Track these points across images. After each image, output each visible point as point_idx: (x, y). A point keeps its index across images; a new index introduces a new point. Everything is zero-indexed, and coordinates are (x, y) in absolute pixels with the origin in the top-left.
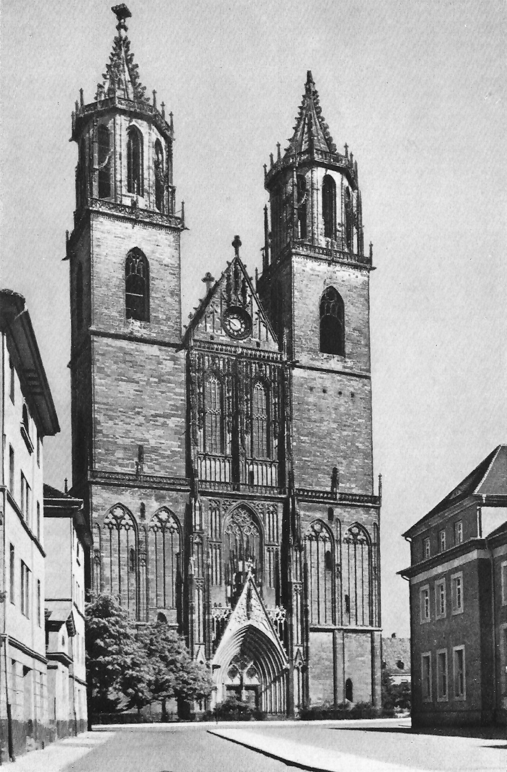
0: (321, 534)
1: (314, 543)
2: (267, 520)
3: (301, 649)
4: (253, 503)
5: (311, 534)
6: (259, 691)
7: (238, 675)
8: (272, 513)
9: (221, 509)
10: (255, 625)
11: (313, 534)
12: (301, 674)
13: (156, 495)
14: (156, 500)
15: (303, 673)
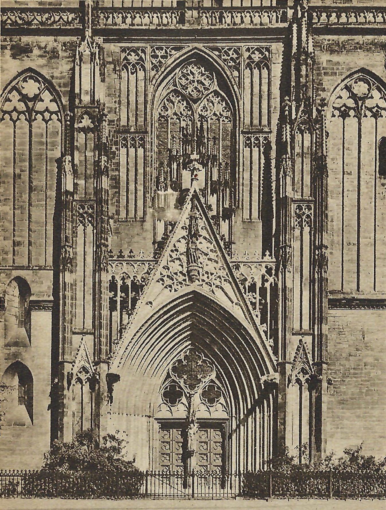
0: (369, 103)
1: (352, 122)
2: (247, 81)
3: (308, 340)
4: (217, 49)
5: (345, 105)
6: (228, 432)
7: (184, 400)
8: (258, 65)
9: (148, 66)
10: (205, 290)
11: (351, 103)
12: (306, 394)
13: (12, 48)
14: (14, 56)
15: (310, 390)
